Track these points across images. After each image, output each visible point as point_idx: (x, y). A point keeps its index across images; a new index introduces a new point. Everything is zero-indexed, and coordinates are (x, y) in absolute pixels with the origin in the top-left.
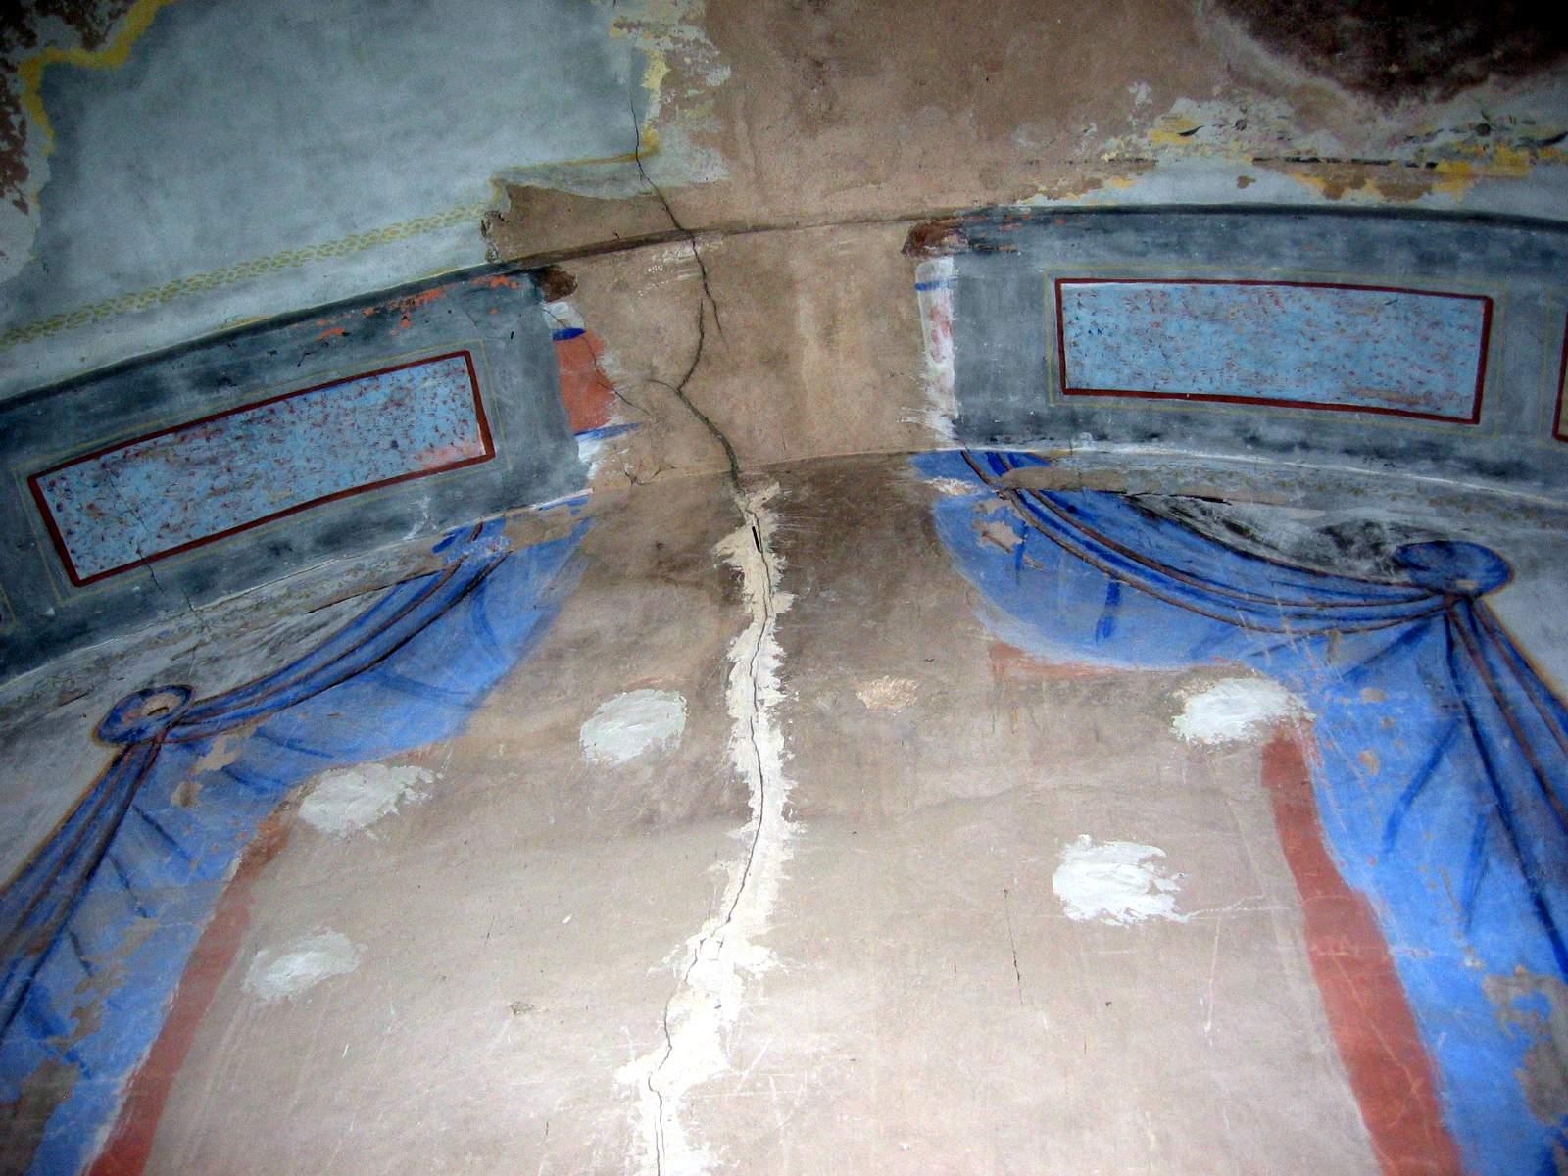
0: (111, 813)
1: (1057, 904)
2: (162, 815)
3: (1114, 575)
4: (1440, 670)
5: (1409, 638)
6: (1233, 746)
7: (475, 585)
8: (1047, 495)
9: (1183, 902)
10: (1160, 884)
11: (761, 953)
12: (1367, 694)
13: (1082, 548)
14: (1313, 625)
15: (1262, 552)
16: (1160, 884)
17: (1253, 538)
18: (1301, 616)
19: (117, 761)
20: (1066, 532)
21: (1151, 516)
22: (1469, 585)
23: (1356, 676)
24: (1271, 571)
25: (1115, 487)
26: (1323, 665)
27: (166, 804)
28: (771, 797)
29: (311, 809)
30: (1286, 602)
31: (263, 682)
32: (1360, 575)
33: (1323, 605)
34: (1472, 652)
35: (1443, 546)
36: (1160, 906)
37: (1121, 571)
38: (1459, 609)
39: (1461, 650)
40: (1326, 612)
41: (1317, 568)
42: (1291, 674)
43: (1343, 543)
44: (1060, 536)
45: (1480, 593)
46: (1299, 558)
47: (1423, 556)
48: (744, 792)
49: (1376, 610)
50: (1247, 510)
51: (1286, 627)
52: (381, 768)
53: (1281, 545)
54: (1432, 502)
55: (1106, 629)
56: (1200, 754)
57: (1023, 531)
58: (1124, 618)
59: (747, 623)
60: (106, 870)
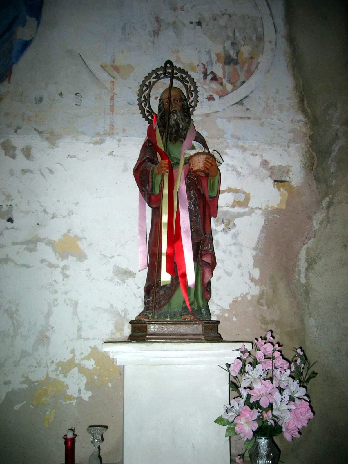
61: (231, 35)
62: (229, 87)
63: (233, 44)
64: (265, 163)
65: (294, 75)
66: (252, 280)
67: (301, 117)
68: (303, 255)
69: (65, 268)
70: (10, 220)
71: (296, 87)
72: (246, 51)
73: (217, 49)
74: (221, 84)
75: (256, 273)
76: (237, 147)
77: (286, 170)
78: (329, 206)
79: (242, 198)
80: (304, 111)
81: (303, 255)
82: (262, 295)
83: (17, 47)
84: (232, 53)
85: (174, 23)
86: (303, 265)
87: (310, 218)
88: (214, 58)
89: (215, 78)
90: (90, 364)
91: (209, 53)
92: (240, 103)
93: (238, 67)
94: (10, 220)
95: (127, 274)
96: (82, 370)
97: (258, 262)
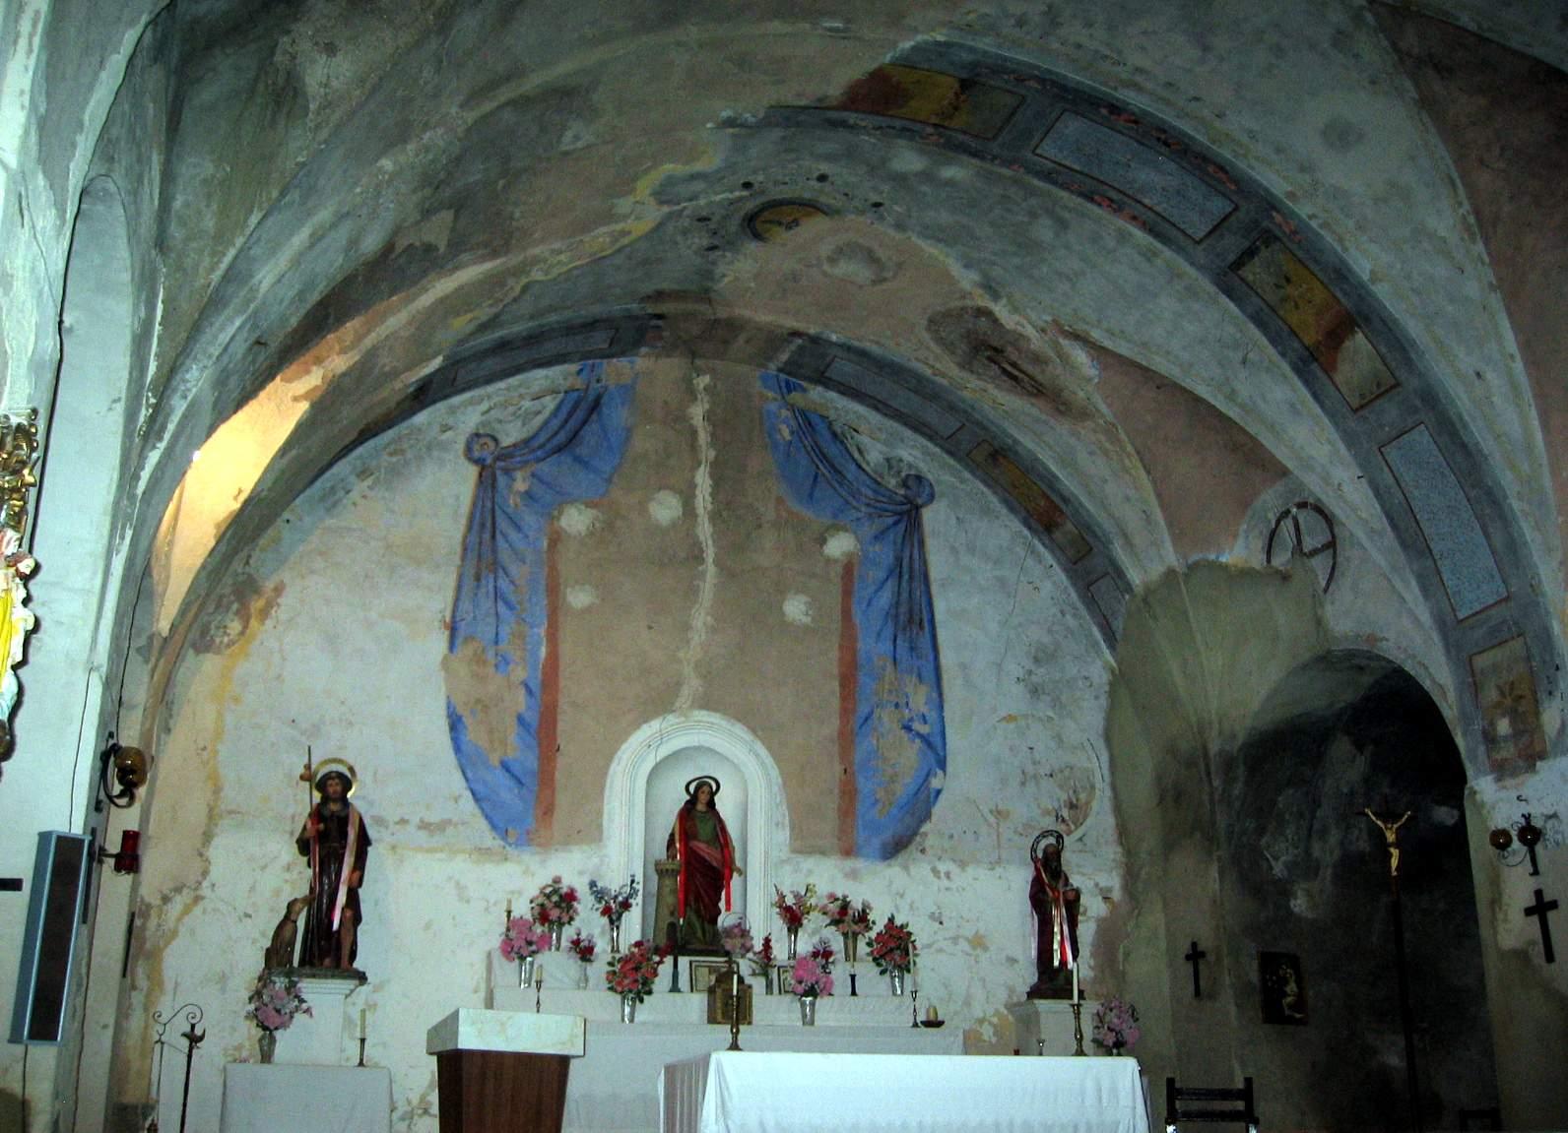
0: (489, 504)
2: (510, 510)
4: (899, 541)
5: (896, 523)
6: (836, 561)
7: (596, 406)
8: (803, 413)
9: (813, 619)
10: (810, 612)
11: (709, 618)
12: (877, 548)
13: (809, 449)
14: (872, 510)
15: (864, 466)
16: (810, 612)
18: (868, 505)
19: (480, 475)
21: (835, 435)
22: (920, 501)
24: (866, 478)
25: (825, 413)
26: (869, 530)
27: (509, 506)
28: (710, 554)
29: (564, 522)
30: (866, 496)
31: (526, 442)
32: (890, 487)
35: (919, 478)
36: (807, 620)
37: (819, 463)
38: (914, 512)
40: (878, 505)
41: (879, 479)
43: (890, 467)
45: (921, 507)
46: (876, 472)
47: (910, 483)
48: (702, 551)
49: (891, 507)
50: (864, 439)
51: (863, 509)
52: (583, 507)
53: (872, 465)
54: (923, 453)
56: (829, 561)
57: (792, 433)
58: (817, 494)
59: (699, 464)
60: (499, 536)
62: (1073, 827)
63: (1075, 792)
64: (1097, 885)
65: (1116, 817)
66: (1090, 967)
67: (1119, 849)
68: (1121, 950)
69: (977, 956)
70: (941, 923)
71: (1117, 825)
72: (1083, 796)
73: (1064, 797)
75: (1092, 963)
76: (1079, 873)
77: (1110, 890)
80: (1121, 844)
81: (1121, 950)
82: (1096, 977)
83: (933, 795)
84: (1074, 801)
86: (1121, 957)
87: (1125, 924)
89: (1063, 820)
90: (995, 1020)
91: (1059, 800)
92: (1080, 839)
94: (941, 923)
95: (1012, 961)
96: (990, 1023)
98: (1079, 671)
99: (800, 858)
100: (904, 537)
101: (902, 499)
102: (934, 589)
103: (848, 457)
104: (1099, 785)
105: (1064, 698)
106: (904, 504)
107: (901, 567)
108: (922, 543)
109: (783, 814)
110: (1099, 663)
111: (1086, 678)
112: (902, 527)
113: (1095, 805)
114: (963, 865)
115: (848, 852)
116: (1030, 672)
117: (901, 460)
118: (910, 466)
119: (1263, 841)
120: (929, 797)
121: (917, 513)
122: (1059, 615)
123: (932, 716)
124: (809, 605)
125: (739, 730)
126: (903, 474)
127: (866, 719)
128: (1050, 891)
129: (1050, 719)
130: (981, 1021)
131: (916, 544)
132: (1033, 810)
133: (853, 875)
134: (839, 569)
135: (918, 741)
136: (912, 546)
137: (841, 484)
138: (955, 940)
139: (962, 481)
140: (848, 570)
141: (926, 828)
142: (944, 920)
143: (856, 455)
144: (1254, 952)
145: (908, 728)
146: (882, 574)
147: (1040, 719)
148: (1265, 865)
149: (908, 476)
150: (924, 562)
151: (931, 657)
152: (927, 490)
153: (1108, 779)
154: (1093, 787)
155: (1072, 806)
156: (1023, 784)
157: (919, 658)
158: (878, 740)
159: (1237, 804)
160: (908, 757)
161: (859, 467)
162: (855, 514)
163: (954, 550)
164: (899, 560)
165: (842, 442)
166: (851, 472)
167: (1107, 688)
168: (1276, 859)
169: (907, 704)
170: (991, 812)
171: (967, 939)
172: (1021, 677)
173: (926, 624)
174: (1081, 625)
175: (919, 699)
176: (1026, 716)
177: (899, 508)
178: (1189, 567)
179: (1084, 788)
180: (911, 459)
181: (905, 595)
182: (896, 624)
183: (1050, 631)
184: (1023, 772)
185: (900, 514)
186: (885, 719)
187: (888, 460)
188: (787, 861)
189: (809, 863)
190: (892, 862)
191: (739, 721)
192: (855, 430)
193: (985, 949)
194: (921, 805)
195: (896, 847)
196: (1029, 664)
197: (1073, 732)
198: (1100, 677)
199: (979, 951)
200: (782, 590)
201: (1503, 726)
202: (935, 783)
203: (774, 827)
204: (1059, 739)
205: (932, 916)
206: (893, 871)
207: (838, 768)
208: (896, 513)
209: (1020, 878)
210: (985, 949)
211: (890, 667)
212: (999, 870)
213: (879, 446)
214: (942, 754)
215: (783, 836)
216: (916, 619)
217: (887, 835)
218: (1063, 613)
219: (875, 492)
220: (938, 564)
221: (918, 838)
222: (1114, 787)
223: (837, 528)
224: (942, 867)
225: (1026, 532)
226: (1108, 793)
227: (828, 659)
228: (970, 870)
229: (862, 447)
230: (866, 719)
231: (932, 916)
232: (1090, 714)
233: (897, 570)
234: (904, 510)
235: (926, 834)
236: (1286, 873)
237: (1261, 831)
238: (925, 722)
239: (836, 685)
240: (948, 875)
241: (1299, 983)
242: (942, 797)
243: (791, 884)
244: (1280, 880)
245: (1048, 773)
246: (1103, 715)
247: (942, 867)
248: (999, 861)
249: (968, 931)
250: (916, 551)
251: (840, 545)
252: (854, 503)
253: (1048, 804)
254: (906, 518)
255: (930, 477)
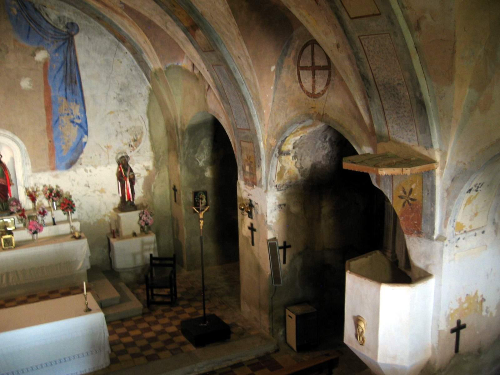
1: (20, 86)
3: (30, 24)
6: (40, 63)
10: (31, 84)
12: (57, 55)
13: (26, 17)
15: (49, 21)
17: (49, 18)
18: (52, 38)
20: (24, 12)
21: (36, 9)
22: (73, 33)
23: (56, 51)
26: (53, 47)
30: (51, 34)
33: (55, 35)
34: (70, 47)
35: (72, 23)
37: (30, 23)
39: (69, 47)
42: (49, 49)
43: (60, 20)
44: (23, 12)
46: (54, 23)
47: (69, 26)
50: (49, 10)
51: (50, 39)
53: (52, 20)
55: (28, 37)
56: (37, 63)
57: (18, 11)
61: (135, 132)
62: (135, 148)
64: (144, 166)
65: (151, 142)
67: (152, 153)
70: (89, 187)
71: (151, 145)
72: (139, 137)
73: (132, 138)
74: (133, 147)
77: (149, 167)
78: (159, 174)
79: (139, 175)
80: (153, 151)
83: (83, 145)
84: (136, 139)
85: (121, 132)
87: (154, 177)
88: (131, 140)
89: (132, 146)
90: (109, 215)
92: (138, 152)
93: (137, 142)
97: (143, 189)
98: (138, 91)
99: (36, 174)
100: (67, 48)
101: (66, 33)
102: (81, 68)
103: (42, 18)
104: (144, 131)
105: (131, 102)
106: (66, 35)
107: (67, 61)
108: (74, 50)
109: (28, 160)
110: (145, 87)
111: (140, 93)
112: (66, 44)
113: (143, 139)
114: (95, 167)
115: (53, 169)
116: (119, 94)
117: (64, 17)
118: (68, 19)
119: (196, 156)
120: (82, 145)
121: (72, 39)
122: (130, 71)
123: (83, 116)
124: (30, 81)
125: (8, 133)
126: (66, 23)
127: (57, 121)
128: (125, 172)
129: (127, 111)
130: (105, 216)
131: (72, 51)
132: (119, 145)
133: (56, 176)
134: (42, 65)
135: (77, 126)
136: (71, 52)
137: (40, 31)
138: (94, 192)
139: (90, 22)
140: (45, 64)
141: (81, 156)
142: (90, 186)
143: (46, 17)
144: (191, 192)
145: (73, 122)
146: (59, 65)
147: (123, 111)
148: (196, 163)
149: (68, 23)
150: (76, 58)
151: (80, 95)
152: (76, 28)
153: (148, 129)
154: (142, 133)
155: (135, 140)
156: (117, 136)
157: (76, 95)
158: (62, 128)
159: (186, 146)
160: (73, 133)
161: (47, 22)
162: (46, 42)
163: (88, 52)
164: (66, 59)
165: (39, 12)
166: (44, 24)
167: (148, 96)
168: (200, 160)
169: (72, 113)
170: (105, 147)
171: (98, 191)
172: (115, 96)
173: (78, 82)
174: (138, 74)
175: (76, 110)
176: (117, 111)
177: (65, 37)
178: (167, 68)
179: (139, 134)
180: (69, 16)
181: (69, 71)
182: (66, 84)
183: (126, 78)
184: (117, 131)
185: (66, 39)
186: (64, 119)
187: (59, 17)
188: (32, 176)
189: (39, 175)
190: (70, 169)
191: (7, 130)
192: (45, 7)
193: (105, 192)
194: (79, 148)
195: (71, 165)
196: (118, 91)
197: (135, 114)
198: (146, 92)
199: (103, 194)
200: (19, 77)
201: (247, 168)
202: (84, 140)
203: (25, 165)
204: (130, 118)
205: (86, 185)
206: (71, 173)
207: (47, 140)
208: (63, 39)
209: (114, 168)
210: (105, 192)
211: (64, 100)
212: (109, 167)
213: (55, 12)
214: (86, 129)
215: (29, 168)
216: (74, 80)
217: (68, 161)
218: (131, 70)
219: (55, 31)
220: (82, 57)
221: (79, 160)
222: (150, 131)
223: (39, 49)
224: (88, 169)
225: (116, 40)
226: (148, 134)
227: (41, 101)
228: (99, 168)
229: (48, 14)
230: (57, 121)
231: (86, 185)
232: (141, 106)
233: (65, 63)
234: (66, 38)
235: (82, 158)
236: (204, 165)
237: (195, 152)
238: (79, 118)
239: (44, 111)
240: (90, 171)
241: (206, 199)
242: (87, 145)
243: (31, 184)
244: (201, 167)
245: (126, 130)
246: (147, 106)
247: (88, 169)
248: (109, 163)
249: (99, 188)
250: (72, 53)
251: (41, 56)
252: (46, 37)
253: (126, 141)
254: (67, 41)
255: (77, 23)
